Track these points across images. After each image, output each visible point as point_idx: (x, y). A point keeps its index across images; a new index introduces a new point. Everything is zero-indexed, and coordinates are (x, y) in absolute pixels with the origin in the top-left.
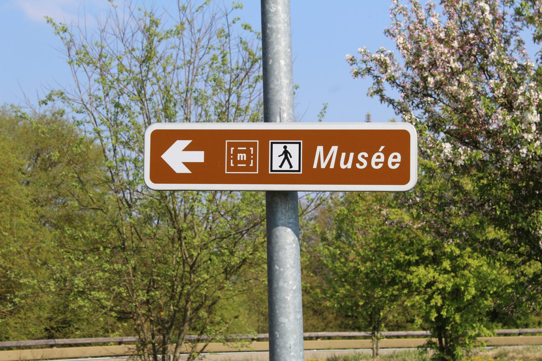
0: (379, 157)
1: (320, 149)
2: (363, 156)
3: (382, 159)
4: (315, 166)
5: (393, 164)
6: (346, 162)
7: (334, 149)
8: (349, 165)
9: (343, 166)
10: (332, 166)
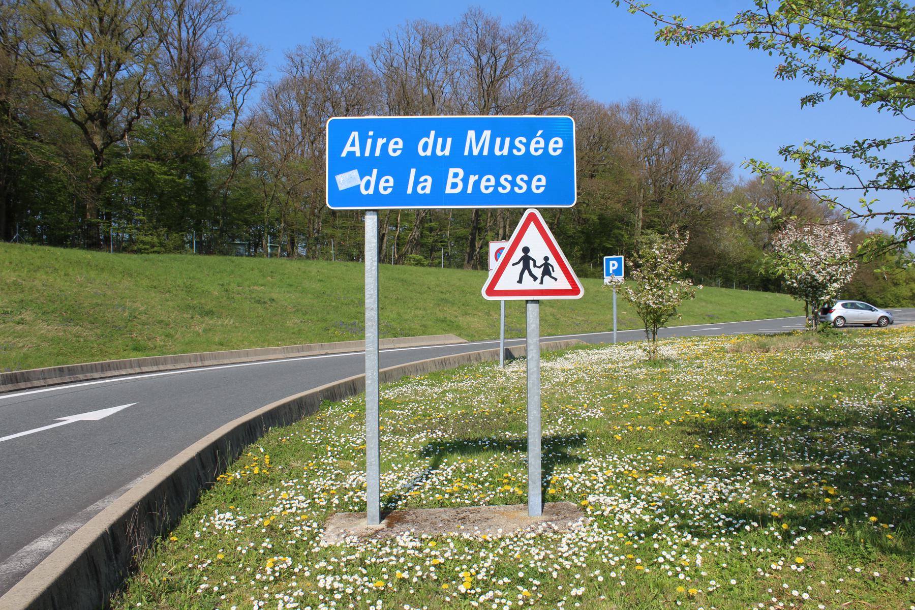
0: (538, 142)
1: (471, 134)
2: (520, 142)
3: (542, 145)
4: (466, 153)
5: (555, 150)
6: (501, 148)
7: (487, 134)
8: (505, 152)
9: (497, 152)
10: (485, 153)
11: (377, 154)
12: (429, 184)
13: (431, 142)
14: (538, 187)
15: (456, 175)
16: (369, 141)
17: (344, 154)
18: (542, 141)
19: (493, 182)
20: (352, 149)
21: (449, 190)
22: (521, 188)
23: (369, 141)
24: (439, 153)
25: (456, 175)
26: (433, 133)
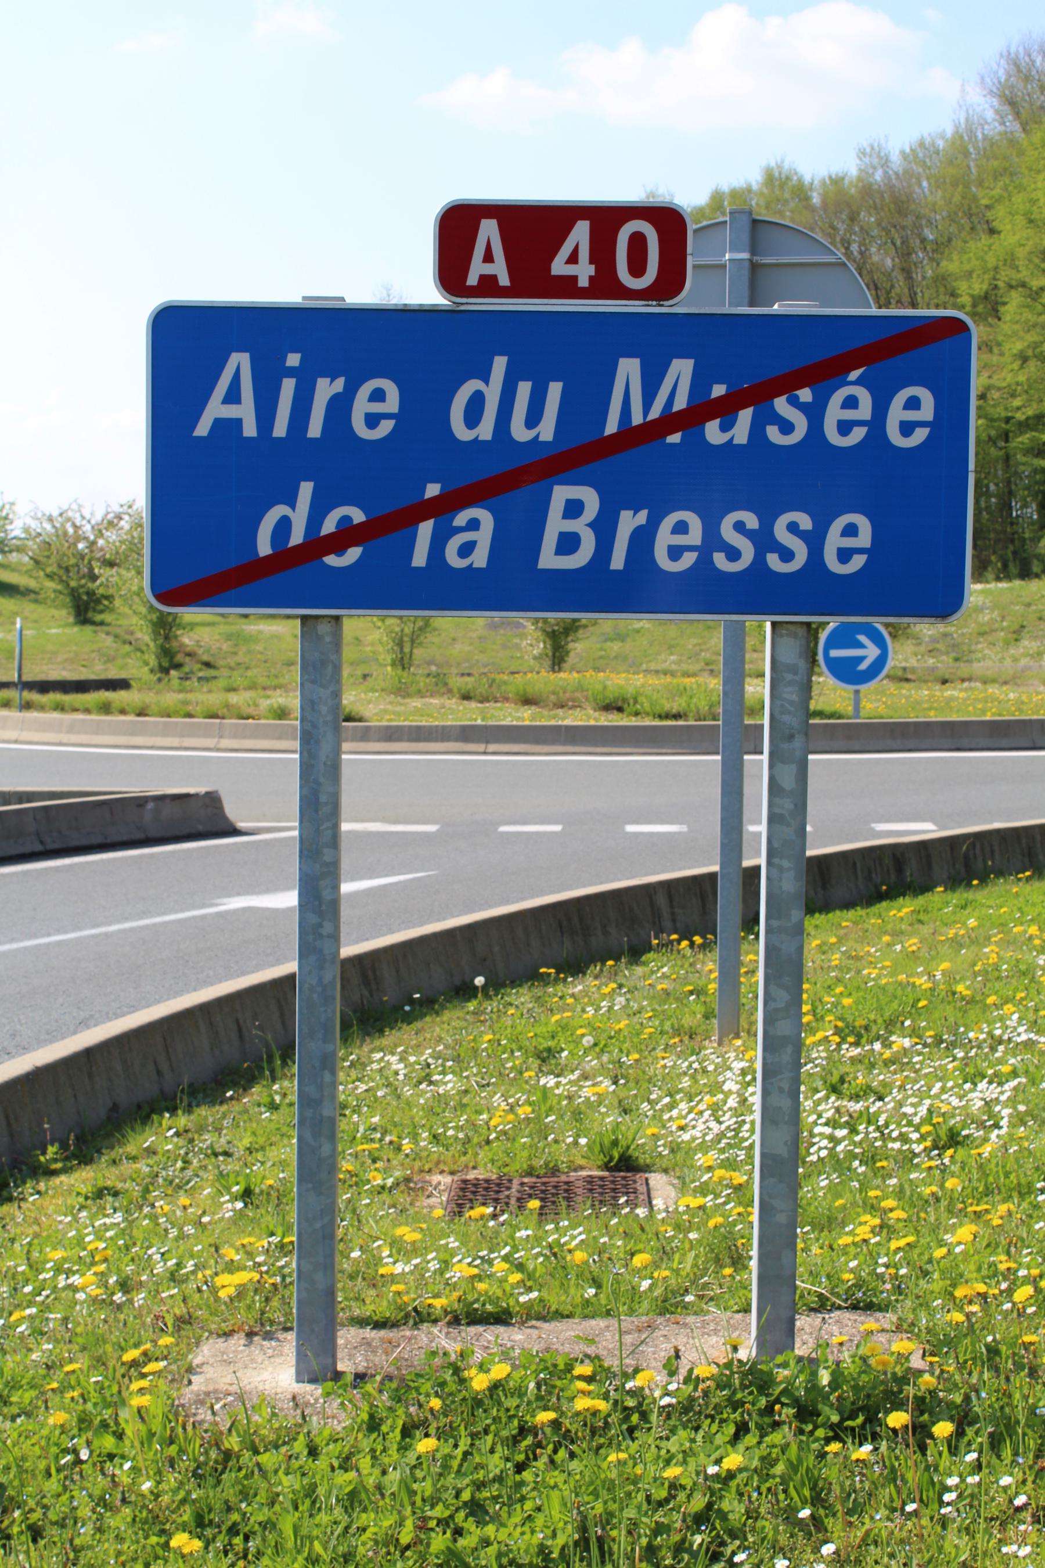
0: (851, 403)
1: (629, 369)
3: (865, 411)
5: (907, 429)
11: (315, 430)
12: (484, 537)
13: (493, 394)
14: (844, 555)
15: (573, 509)
16: (288, 386)
17: (202, 429)
18: (864, 397)
19: (695, 536)
20: (230, 412)
21: (549, 559)
22: (787, 555)
23: (288, 386)
24: (520, 432)
25: (573, 509)
26: (500, 365)
